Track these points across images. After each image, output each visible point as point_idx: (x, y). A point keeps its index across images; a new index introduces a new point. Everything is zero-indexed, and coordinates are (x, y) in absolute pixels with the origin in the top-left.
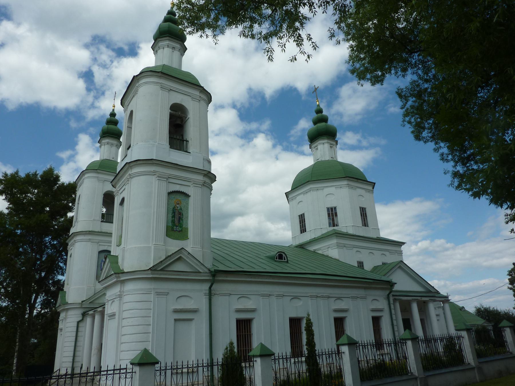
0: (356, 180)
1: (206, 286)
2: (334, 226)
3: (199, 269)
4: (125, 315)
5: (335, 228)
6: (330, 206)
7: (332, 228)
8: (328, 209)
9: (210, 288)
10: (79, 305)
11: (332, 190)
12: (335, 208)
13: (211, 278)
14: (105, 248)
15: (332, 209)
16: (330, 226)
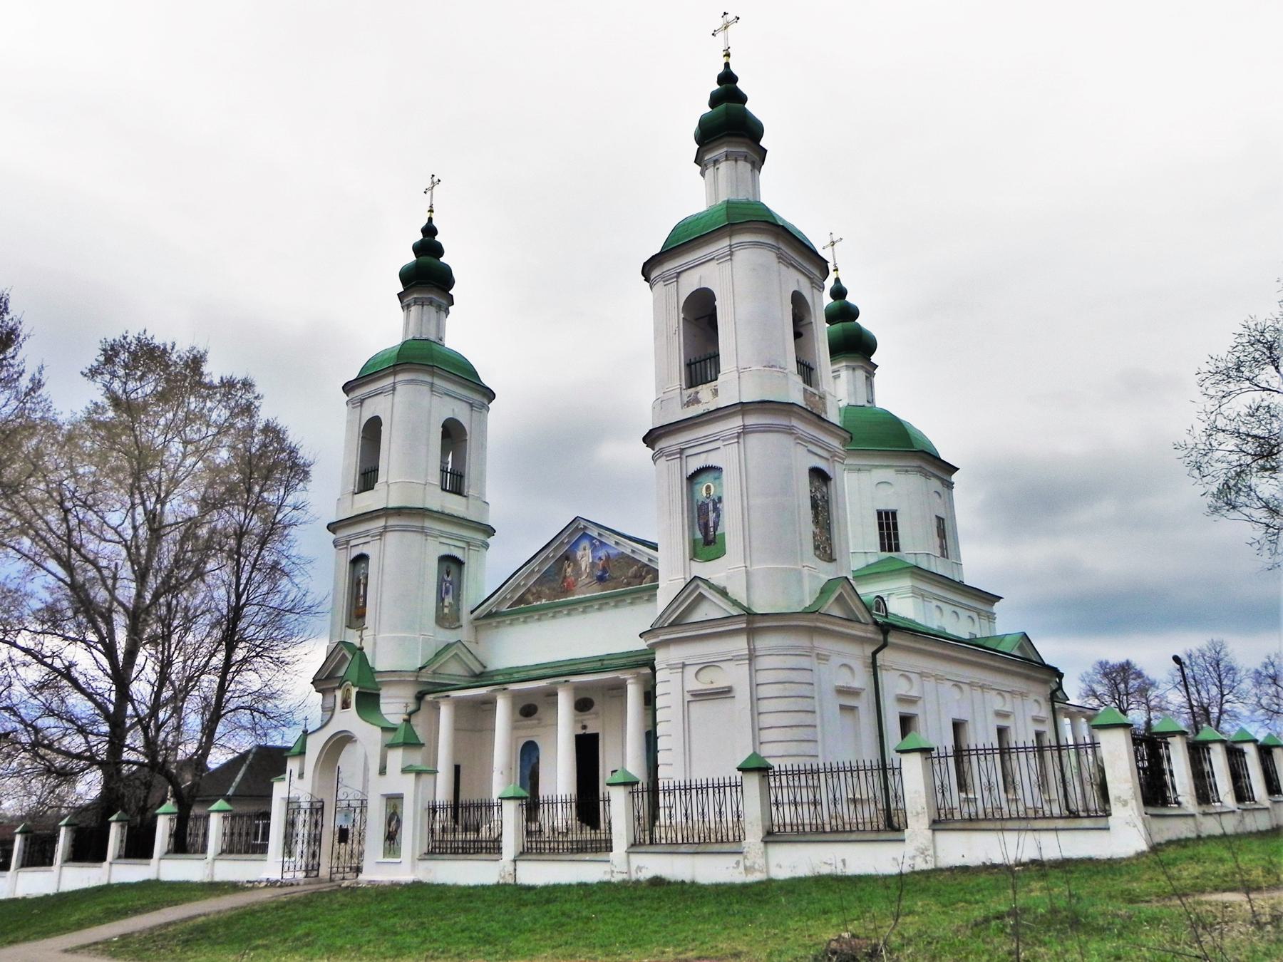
0: (931, 459)
1: (869, 650)
2: (890, 550)
3: (860, 617)
4: (763, 691)
5: (894, 554)
6: (883, 507)
7: (887, 554)
8: (879, 513)
9: (874, 654)
10: (410, 676)
11: (888, 474)
12: (894, 513)
13: (881, 638)
14: (458, 553)
15: (887, 513)
16: (883, 549)
